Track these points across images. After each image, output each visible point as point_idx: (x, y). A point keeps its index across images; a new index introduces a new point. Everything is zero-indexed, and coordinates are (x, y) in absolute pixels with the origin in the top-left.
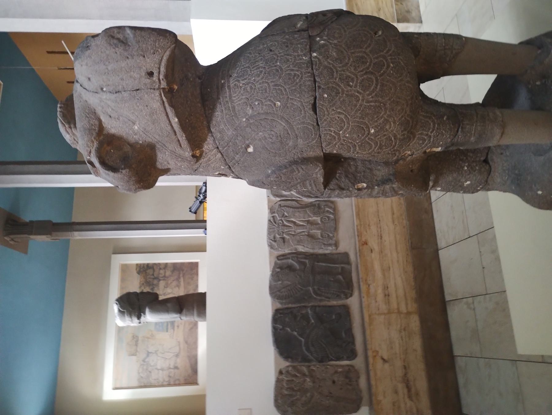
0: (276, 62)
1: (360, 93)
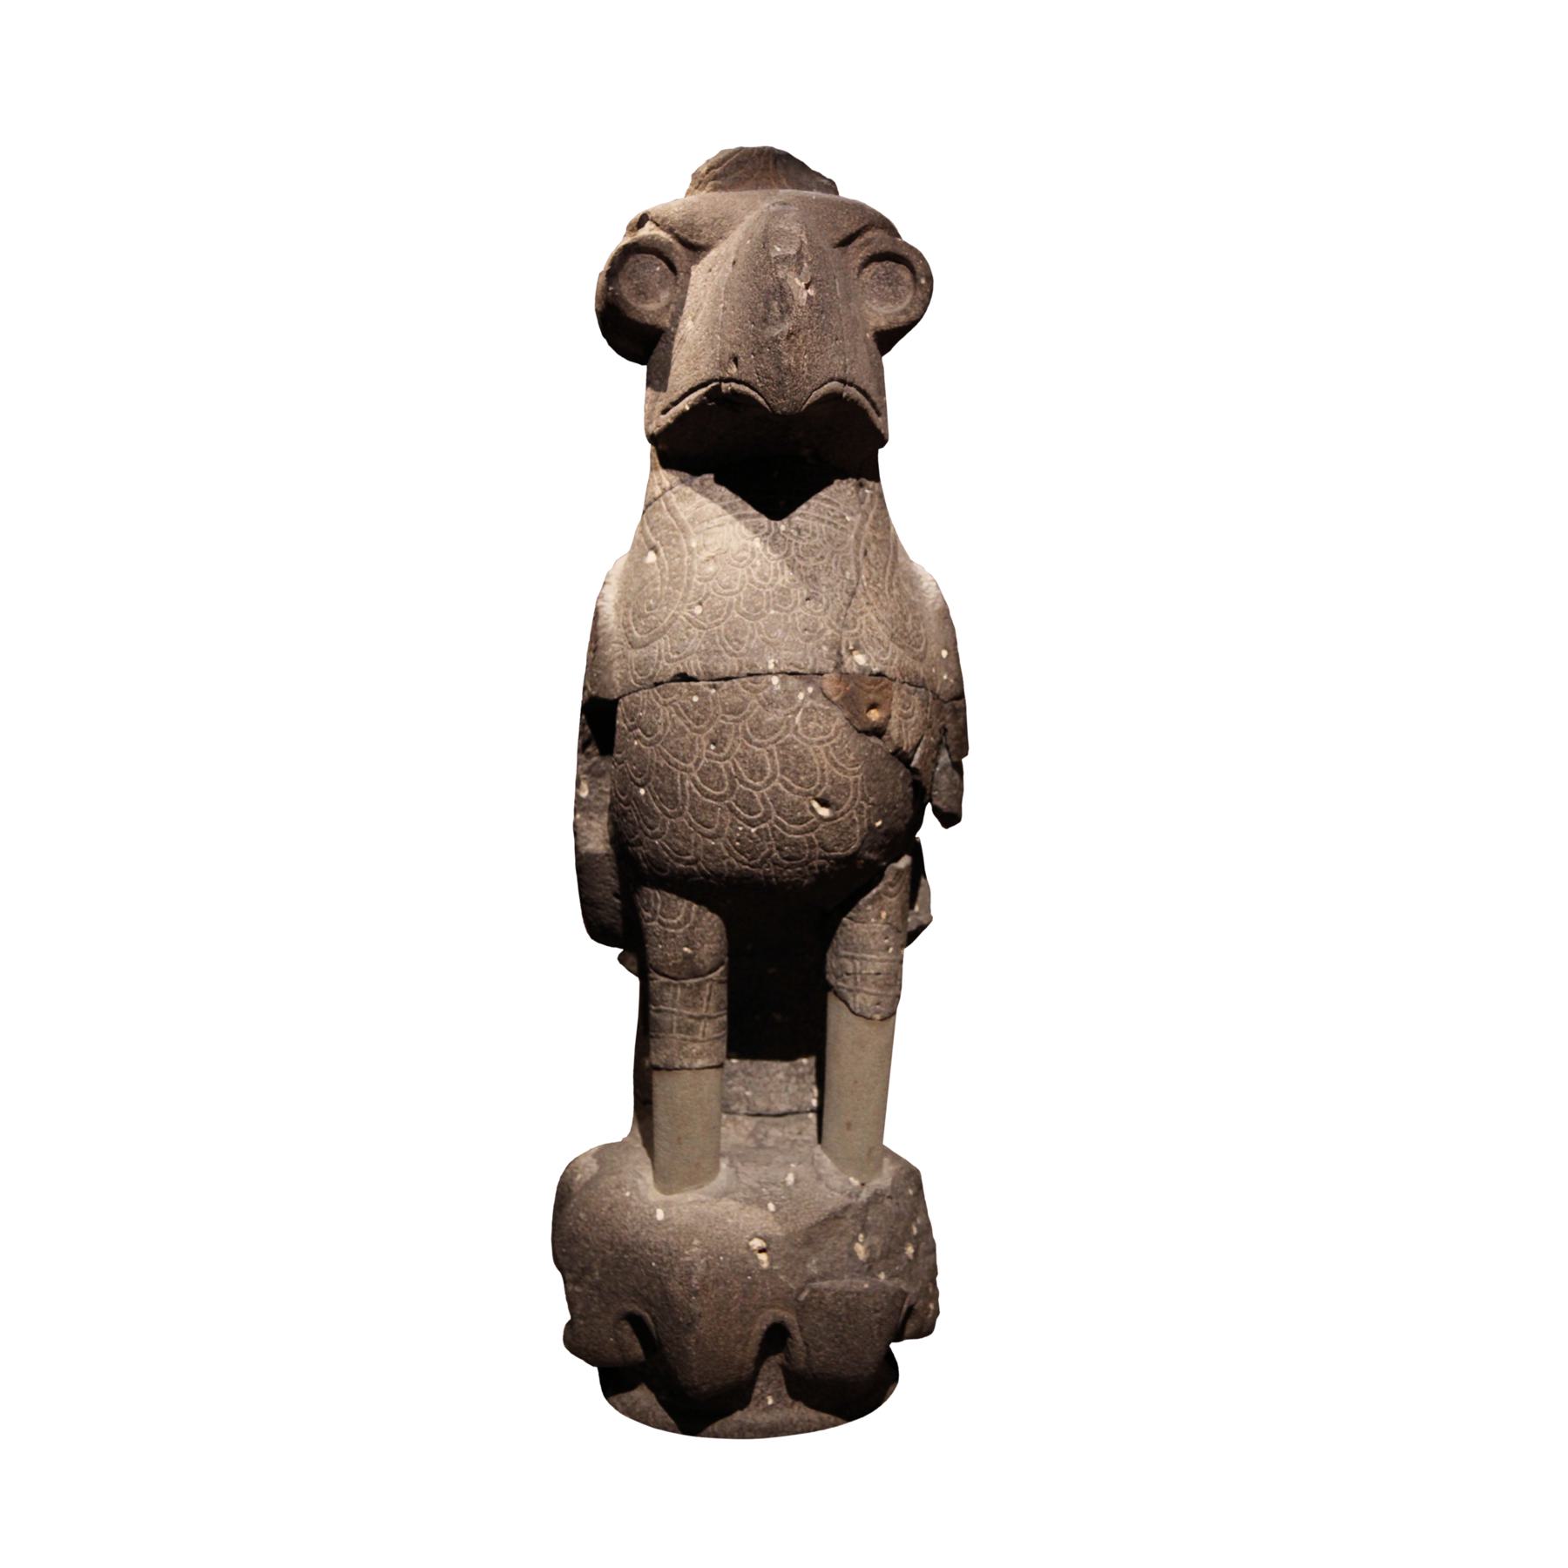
0: (776, 609)
1: (696, 764)
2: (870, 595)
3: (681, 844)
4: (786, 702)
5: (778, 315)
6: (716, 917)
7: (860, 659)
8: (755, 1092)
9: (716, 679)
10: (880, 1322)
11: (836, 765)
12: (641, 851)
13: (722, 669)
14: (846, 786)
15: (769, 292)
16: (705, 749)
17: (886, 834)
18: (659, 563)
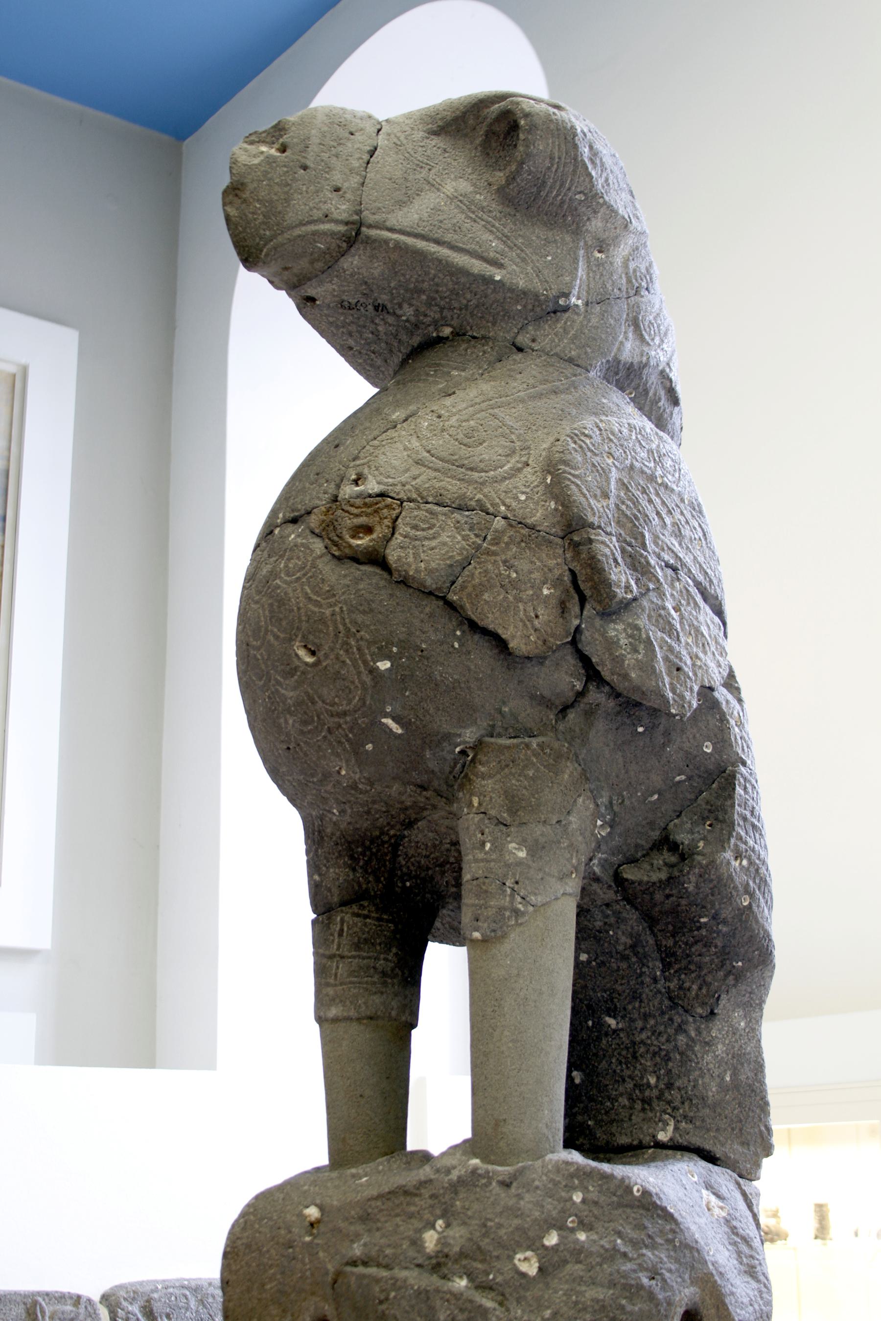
14: (322, 620)
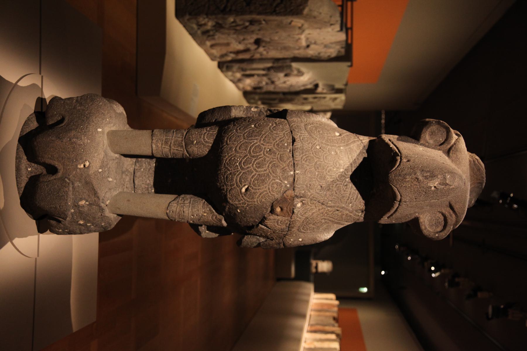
1: (262, 144)
2: (323, 210)
3: (234, 139)
4: (284, 176)
5: (425, 175)
6: (207, 153)
7: (299, 205)
8: (143, 172)
9: (293, 152)
10: (56, 208)
11: (260, 194)
12: (231, 126)
13: (297, 154)
14: (253, 198)
15: (433, 172)
16: (268, 147)
17: (235, 214)
18: (335, 136)
